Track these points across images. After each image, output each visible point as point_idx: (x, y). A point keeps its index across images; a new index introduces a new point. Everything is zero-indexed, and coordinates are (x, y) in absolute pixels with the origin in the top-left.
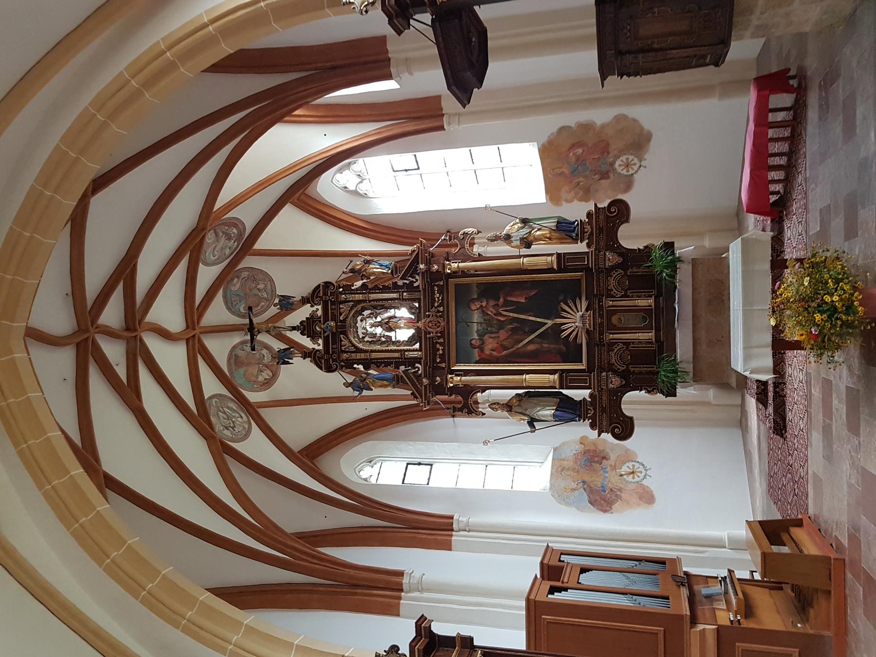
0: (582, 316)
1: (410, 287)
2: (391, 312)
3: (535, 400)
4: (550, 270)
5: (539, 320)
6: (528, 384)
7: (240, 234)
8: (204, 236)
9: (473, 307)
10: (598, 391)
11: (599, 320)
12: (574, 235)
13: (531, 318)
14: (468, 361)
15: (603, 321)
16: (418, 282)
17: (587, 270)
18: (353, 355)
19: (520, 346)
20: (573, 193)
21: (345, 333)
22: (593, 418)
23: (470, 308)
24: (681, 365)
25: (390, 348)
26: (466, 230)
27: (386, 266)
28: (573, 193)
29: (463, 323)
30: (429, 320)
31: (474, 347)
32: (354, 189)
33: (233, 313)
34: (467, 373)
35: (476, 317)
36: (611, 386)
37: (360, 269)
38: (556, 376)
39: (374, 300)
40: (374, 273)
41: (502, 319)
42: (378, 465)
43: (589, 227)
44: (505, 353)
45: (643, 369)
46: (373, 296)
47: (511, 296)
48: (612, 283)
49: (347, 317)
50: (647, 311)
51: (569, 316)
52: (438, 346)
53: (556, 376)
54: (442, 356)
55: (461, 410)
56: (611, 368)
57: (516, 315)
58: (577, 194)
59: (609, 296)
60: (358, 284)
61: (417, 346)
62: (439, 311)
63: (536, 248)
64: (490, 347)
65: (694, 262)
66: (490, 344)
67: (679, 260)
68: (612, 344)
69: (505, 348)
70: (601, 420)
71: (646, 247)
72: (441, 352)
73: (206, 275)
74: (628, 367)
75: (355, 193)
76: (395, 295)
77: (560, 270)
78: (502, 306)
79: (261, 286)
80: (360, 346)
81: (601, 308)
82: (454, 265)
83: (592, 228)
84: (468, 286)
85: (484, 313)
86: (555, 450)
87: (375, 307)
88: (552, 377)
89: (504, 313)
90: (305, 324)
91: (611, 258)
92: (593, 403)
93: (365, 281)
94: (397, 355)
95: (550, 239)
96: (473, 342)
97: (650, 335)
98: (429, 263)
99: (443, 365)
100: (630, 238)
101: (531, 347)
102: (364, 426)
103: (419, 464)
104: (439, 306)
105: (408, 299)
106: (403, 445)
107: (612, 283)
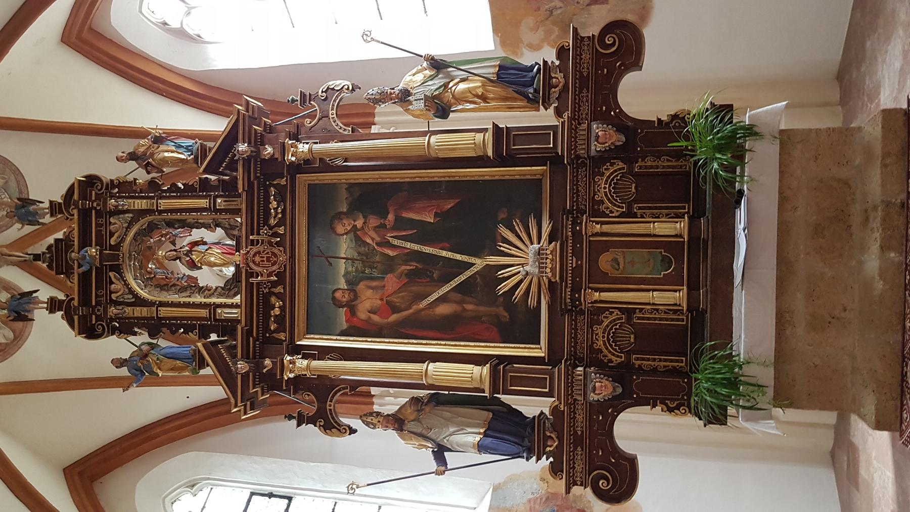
0: (539, 253)
2: (197, 234)
3: (446, 412)
4: (480, 161)
5: (458, 257)
6: (430, 382)
9: (340, 229)
10: (567, 404)
11: (572, 262)
12: (531, 90)
13: (444, 253)
14: (327, 330)
15: (581, 265)
17: (554, 160)
18: (128, 310)
19: (424, 303)
20: (541, 32)
21: (118, 269)
22: (557, 455)
23: (333, 229)
24: (747, 370)
25: (191, 300)
26: (331, 84)
28: (541, 32)
29: (321, 258)
30: (255, 250)
31: (339, 304)
32: (179, 26)
34: (323, 353)
35: (345, 247)
36: (593, 397)
37: (144, 154)
38: (486, 369)
40: (165, 161)
41: (391, 253)
42: (206, 491)
43: (560, 76)
44: (394, 317)
45: (662, 362)
46: (164, 204)
47: (411, 210)
48: (603, 187)
49: (123, 240)
50: (671, 246)
51: (514, 251)
52: (273, 299)
53: (486, 369)
54: (280, 320)
55: (312, 420)
56: (595, 361)
57: (416, 247)
58: (548, 33)
59: (596, 212)
61: (237, 299)
62: (276, 235)
63: (455, 120)
64: (367, 305)
65: (786, 138)
66: (368, 300)
67: (751, 131)
68: (597, 312)
69: (395, 309)
70: (572, 460)
71: (675, 117)
72: (277, 311)
74: (628, 358)
75: (181, 33)
76: (203, 203)
77: (502, 158)
78: (394, 228)
80: (143, 294)
81: (577, 235)
83: (566, 77)
84: (331, 188)
85: (359, 240)
86: (496, 489)
87: (170, 224)
88: (477, 370)
89: (396, 242)
91: (603, 136)
92: (557, 427)
93: (154, 175)
94: (204, 313)
95: (484, 98)
96: (338, 295)
97: (678, 297)
98: (258, 142)
99: (282, 336)
100: (641, 96)
101: (444, 309)
102: (168, 431)
103: (271, 495)
104: (278, 225)
105: (226, 211)
106: (244, 462)
107: (603, 187)
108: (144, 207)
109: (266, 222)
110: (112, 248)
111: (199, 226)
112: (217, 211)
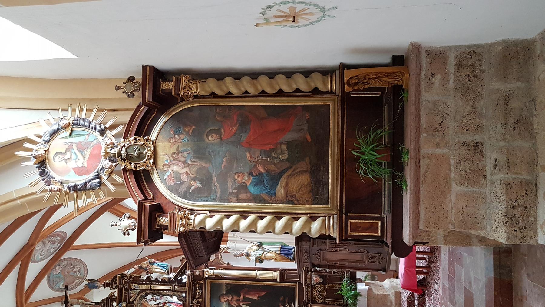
1: (180, 283)
7: (63, 239)
8: (33, 249)
9: (223, 300)
16: (185, 279)
23: (220, 300)
27: (164, 267)
33: (54, 290)
39: (154, 290)
46: (154, 287)
47: (248, 294)
48: (316, 293)
49: (135, 300)
60: (144, 277)
62: (199, 302)
73: (33, 269)
76: (169, 288)
78: (243, 301)
79: (77, 269)
82: (211, 272)
84: (220, 285)
90: (105, 302)
95: (275, 259)
104: (199, 298)
105: (178, 291)
108: (145, 288)
109: (195, 296)
110: (131, 303)
111: (166, 295)
112: (175, 291)
